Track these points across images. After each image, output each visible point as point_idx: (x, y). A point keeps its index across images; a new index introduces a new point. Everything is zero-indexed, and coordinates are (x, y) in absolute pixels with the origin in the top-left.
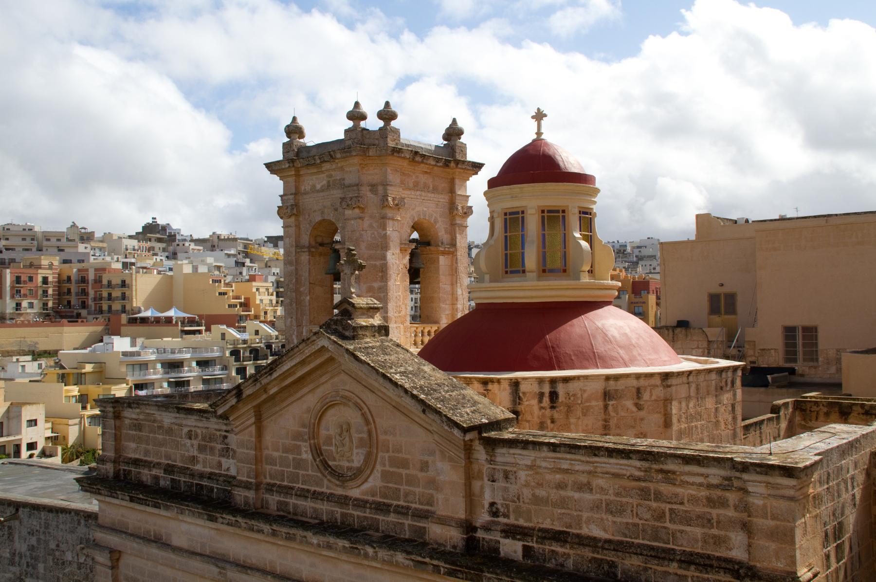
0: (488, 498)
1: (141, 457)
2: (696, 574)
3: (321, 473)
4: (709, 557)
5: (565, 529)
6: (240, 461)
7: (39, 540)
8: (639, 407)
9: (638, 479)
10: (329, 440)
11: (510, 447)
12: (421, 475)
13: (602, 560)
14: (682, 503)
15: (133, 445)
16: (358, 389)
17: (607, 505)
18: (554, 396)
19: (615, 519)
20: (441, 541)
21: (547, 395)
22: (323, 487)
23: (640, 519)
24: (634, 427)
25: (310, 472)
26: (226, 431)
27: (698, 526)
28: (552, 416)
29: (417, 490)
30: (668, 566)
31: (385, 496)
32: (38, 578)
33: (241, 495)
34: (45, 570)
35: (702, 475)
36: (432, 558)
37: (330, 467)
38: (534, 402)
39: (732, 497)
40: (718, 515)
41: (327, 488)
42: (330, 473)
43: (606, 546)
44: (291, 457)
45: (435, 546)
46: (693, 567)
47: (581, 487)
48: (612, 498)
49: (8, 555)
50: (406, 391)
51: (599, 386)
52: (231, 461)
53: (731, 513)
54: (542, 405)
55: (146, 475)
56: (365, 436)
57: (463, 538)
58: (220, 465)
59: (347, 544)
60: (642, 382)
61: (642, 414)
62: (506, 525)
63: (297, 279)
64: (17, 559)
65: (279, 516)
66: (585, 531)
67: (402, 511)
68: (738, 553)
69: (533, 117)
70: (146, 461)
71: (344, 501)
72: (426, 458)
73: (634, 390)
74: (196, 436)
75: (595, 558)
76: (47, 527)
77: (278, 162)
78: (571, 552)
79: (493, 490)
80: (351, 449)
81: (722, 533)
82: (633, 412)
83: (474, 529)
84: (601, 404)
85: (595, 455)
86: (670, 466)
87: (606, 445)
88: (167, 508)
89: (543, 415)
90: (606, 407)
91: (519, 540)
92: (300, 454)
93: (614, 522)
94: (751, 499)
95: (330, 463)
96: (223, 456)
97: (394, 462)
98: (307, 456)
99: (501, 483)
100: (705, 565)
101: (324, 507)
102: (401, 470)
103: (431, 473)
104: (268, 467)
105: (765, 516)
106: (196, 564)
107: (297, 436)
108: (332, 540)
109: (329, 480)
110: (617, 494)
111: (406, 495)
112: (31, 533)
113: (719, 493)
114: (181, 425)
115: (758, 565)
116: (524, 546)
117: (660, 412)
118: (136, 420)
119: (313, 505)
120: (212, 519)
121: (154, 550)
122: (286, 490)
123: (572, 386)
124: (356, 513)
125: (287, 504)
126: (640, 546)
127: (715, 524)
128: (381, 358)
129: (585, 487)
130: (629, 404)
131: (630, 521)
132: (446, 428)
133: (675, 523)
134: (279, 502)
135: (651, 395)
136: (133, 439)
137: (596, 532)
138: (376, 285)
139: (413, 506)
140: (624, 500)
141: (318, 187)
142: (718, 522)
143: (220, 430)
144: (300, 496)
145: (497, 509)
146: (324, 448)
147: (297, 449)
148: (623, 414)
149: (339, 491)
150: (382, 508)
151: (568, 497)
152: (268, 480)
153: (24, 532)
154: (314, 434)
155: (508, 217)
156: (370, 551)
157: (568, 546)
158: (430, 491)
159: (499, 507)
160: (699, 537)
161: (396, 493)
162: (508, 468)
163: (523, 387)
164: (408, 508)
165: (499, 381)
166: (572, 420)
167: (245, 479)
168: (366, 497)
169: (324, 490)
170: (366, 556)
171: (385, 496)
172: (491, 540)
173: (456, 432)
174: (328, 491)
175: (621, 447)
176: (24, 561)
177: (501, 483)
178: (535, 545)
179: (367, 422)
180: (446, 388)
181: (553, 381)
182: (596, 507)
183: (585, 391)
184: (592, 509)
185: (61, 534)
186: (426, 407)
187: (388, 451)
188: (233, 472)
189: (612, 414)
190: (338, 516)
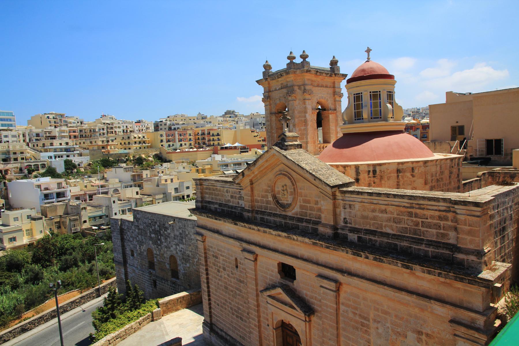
0: (343, 216)
1: (211, 200)
2: (433, 250)
3: (276, 206)
4: (439, 242)
5: (375, 229)
6: (245, 201)
7: (182, 231)
8: (413, 176)
9: (408, 207)
11: (352, 194)
12: (315, 206)
13: (391, 243)
14: (427, 219)
15: (207, 196)
16: (290, 171)
17: (394, 219)
18: (374, 172)
19: (397, 225)
20: (324, 234)
21: (371, 171)
22: (277, 211)
23: (408, 225)
24: (411, 185)
25: (272, 206)
26: (240, 189)
27: (434, 229)
28: (374, 181)
29: (314, 213)
30: (420, 246)
31: (301, 215)
32: (183, 244)
33: (246, 214)
34: (186, 241)
35: (436, 206)
36: (319, 241)
37: (279, 203)
38: (366, 175)
39: (450, 215)
40: (443, 224)
41: (279, 212)
42: (280, 206)
43: (393, 237)
44: (265, 199)
45: (321, 236)
46: (431, 247)
48: (396, 216)
49: (173, 236)
50: (307, 171)
51: (395, 168)
52: (242, 201)
53: (450, 223)
54: (369, 176)
55: (213, 207)
56: (292, 190)
57: (332, 233)
58: (238, 203)
60: (415, 165)
61: (414, 179)
62: (351, 227)
63: (271, 128)
64: (176, 237)
65: (261, 223)
66: (384, 230)
67: (308, 221)
68: (452, 241)
69: (366, 51)
70: (212, 202)
71: (285, 217)
72: (317, 199)
73: (411, 169)
74: (229, 192)
75: (388, 242)
76: (185, 226)
77: (261, 80)
78: (378, 239)
79: (345, 213)
80: (288, 196)
81: (446, 232)
82: (410, 178)
83: (337, 229)
84: (396, 175)
85: (388, 197)
86: (421, 202)
87: (393, 193)
88: (220, 220)
89: (370, 180)
90: (398, 176)
91: (356, 234)
92: (268, 198)
93: (397, 227)
94: (459, 217)
95: (280, 202)
96: (240, 199)
97: (305, 201)
98: (270, 199)
99: (348, 210)
100: (437, 246)
101: (278, 219)
102: (307, 205)
103: (319, 206)
104: (256, 204)
105: (465, 225)
106: (231, 241)
107: (267, 191)
108: (280, 233)
109: (279, 209)
110: (398, 215)
111: (310, 215)
112: (180, 228)
113: (444, 213)
114: (224, 187)
115: (461, 246)
116: (358, 236)
117: (423, 178)
118: (208, 186)
119: (273, 219)
120: (236, 224)
121: (216, 235)
122: (263, 213)
123: (383, 168)
124: (290, 222)
125: (264, 218)
126: (408, 237)
127: (442, 228)
128: (298, 157)
129: (385, 211)
130: (408, 174)
131: (404, 226)
132: (324, 186)
133: (424, 227)
134: (261, 218)
135: (418, 171)
136: (207, 193)
137: (389, 231)
138: (303, 128)
139: (313, 219)
140: (401, 217)
141: (277, 89)
142: (444, 227)
143: (238, 189)
144: (269, 215)
145: (347, 221)
146: (277, 195)
147: (267, 196)
148: (405, 179)
149: (284, 213)
150: (300, 220)
151: (377, 216)
152: (257, 209)
153: (178, 228)
155: (355, 96)
156: (295, 237)
157: (377, 237)
158: (319, 213)
159: (348, 220)
160: (435, 233)
162: (351, 203)
163: (361, 168)
164: (310, 220)
165: (350, 166)
166: (383, 182)
167: (248, 208)
168: (294, 216)
169: (278, 213)
170: (294, 239)
171: (301, 215)
172: (344, 234)
173: (328, 188)
174: (279, 213)
175: (399, 194)
176: (178, 238)
177: (348, 210)
178: (363, 236)
179: (293, 185)
180: (325, 170)
181: (374, 165)
182: (389, 220)
183: (388, 169)
184: (387, 221)
185: (189, 228)
186: (316, 178)
187: (302, 197)
188: (243, 206)
189: (401, 179)
190: (283, 223)
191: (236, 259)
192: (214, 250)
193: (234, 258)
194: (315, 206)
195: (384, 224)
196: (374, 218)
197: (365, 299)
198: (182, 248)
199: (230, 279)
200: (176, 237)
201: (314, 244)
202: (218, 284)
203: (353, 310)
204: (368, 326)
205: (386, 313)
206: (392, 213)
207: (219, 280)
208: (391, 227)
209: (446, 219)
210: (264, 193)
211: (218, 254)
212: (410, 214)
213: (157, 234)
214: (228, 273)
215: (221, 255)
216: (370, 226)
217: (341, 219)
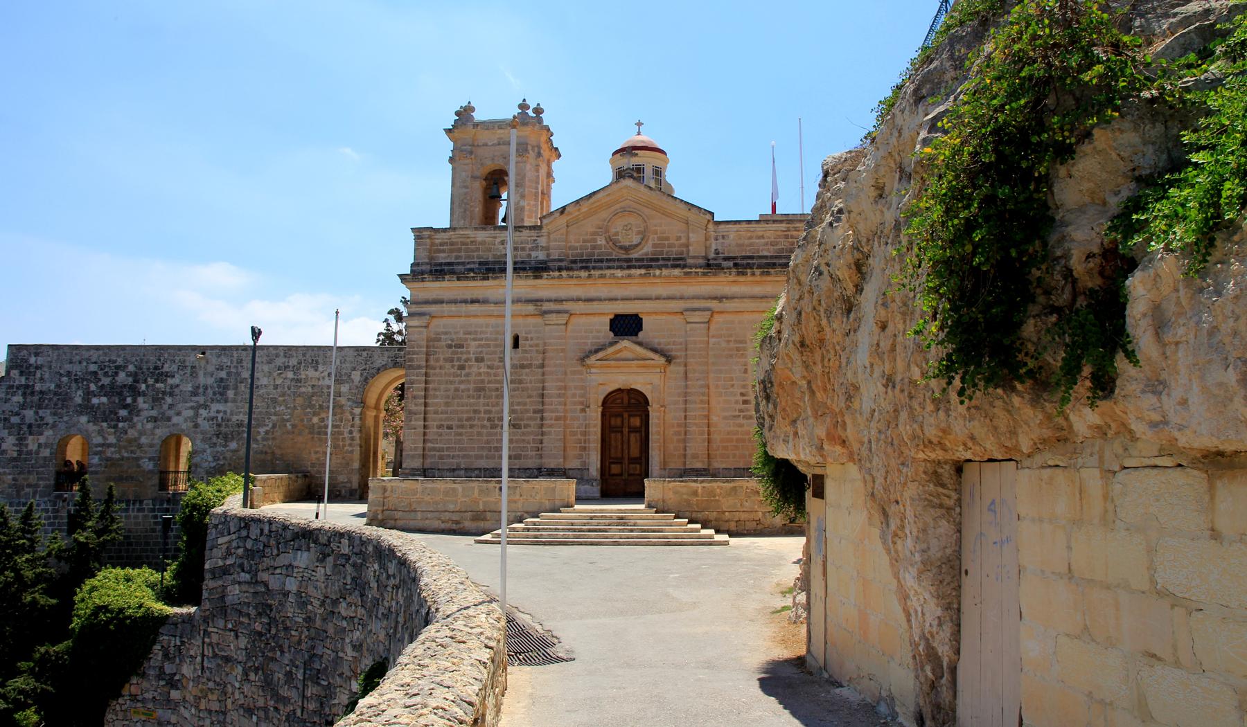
0: (714, 247)
7: (229, 374)
9: (784, 231)
10: (617, 234)
12: (676, 242)
25: (603, 250)
29: (674, 249)
44: (589, 244)
58: (530, 256)
59: (643, 271)
66: (761, 254)
79: (716, 244)
83: (709, 260)
92: (596, 242)
98: (601, 241)
99: (721, 240)
111: (667, 252)
112: (220, 368)
129: (763, 237)
137: (766, 254)
149: (625, 256)
154: (607, 231)
156: (658, 272)
170: (654, 276)
177: (721, 240)
182: (766, 244)
187: (656, 234)
192: (454, 336)
194: (676, 242)
195: (761, 248)
196: (751, 245)
198: (218, 412)
199: (492, 371)
200: (201, 390)
201: (686, 274)
202: (457, 390)
204: (745, 349)
206: (769, 238)
207: (461, 382)
208: (768, 250)
210: (589, 237)
211: (466, 340)
212: (787, 237)
213: (120, 394)
214: (489, 363)
215: (475, 340)
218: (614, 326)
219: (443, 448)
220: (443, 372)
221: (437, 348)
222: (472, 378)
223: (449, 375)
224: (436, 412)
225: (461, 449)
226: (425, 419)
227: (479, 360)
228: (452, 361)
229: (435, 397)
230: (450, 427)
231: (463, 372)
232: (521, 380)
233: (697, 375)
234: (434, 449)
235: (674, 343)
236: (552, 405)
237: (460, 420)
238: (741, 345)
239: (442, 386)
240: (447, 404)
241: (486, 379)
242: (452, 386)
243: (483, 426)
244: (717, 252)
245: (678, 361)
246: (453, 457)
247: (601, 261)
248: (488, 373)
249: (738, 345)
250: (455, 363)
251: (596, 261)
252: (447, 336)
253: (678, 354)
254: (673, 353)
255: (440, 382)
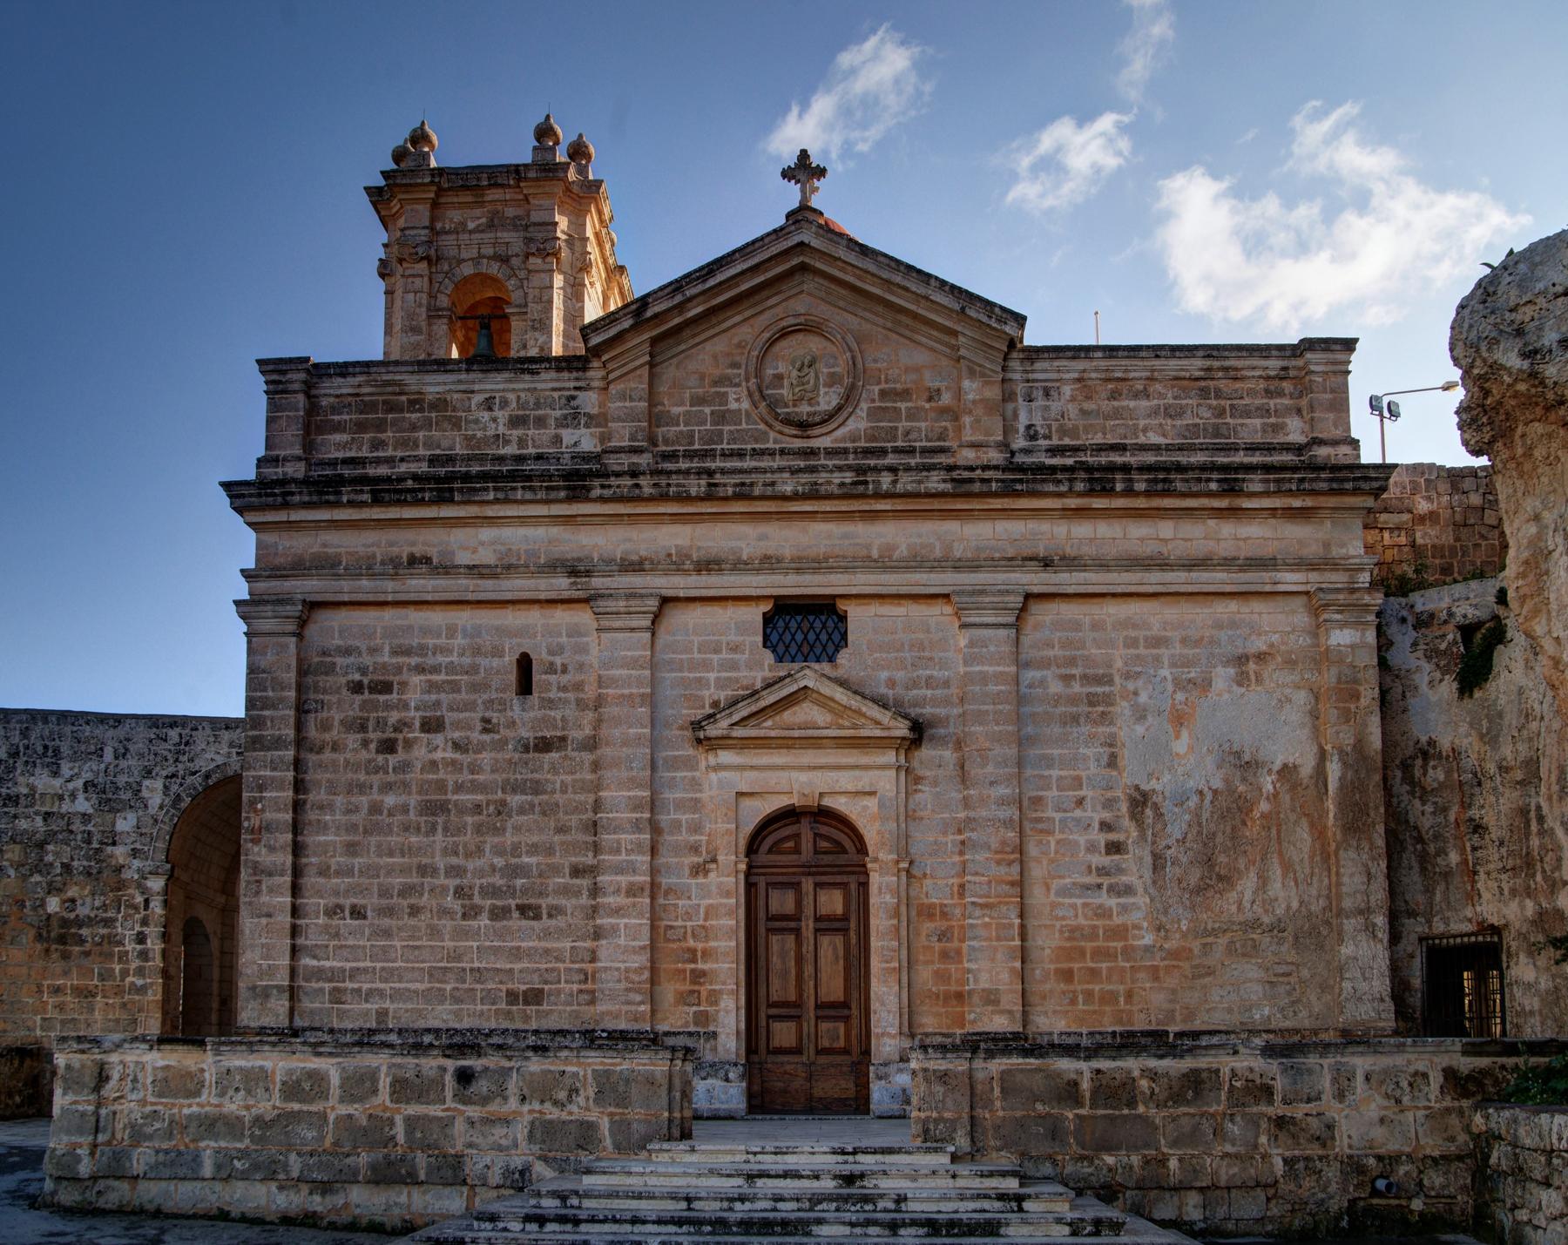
47: (1136, 396)
66: (1142, 440)
79: (1030, 411)
83: (1013, 453)
98: (737, 400)
99: (1040, 402)
110: (1175, 398)
113: (1277, 382)
149: (798, 444)
161: (892, 434)
171: (874, 438)
177: (1040, 402)
182: (1155, 412)
184: (1149, 416)
187: (879, 383)
191: (525, 664)
193: (510, 659)
195: (1142, 423)
197: (1096, 626)
202: (375, 809)
203: (1063, 671)
204: (1108, 700)
205: (1158, 642)
207: (387, 788)
209: (1281, 394)
214: (456, 735)
216: (1104, 434)
217: (1017, 431)
218: (774, 638)
219: (343, 970)
220: (341, 758)
221: (325, 692)
222: (414, 775)
223: (356, 767)
224: (324, 872)
225: (387, 976)
226: (296, 890)
227: (432, 725)
228: (363, 728)
229: (324, 828)
230: (357, 913)
231: (392, 760)
232: (538, 782)
233: (990, 769)
234: (319, 974)
235: (929, 682)
236: (618, 851)
237: (384, 893)
238: (1099, 690)
239: (339, 800)
240: (352, 849)
241: (451, 780)
242: (364, 799)
243: (445, 912)
244: (1032, 435)
245: (942, 731)
246: (370, 994)
247: (740, 454)
248: (453, 762)
249: (1092, 690)
250: (372, 735)
251: (725, 455)
252: (350, 660)
253: (941, 711)
254: (928, 710)
255: (332, 789)
